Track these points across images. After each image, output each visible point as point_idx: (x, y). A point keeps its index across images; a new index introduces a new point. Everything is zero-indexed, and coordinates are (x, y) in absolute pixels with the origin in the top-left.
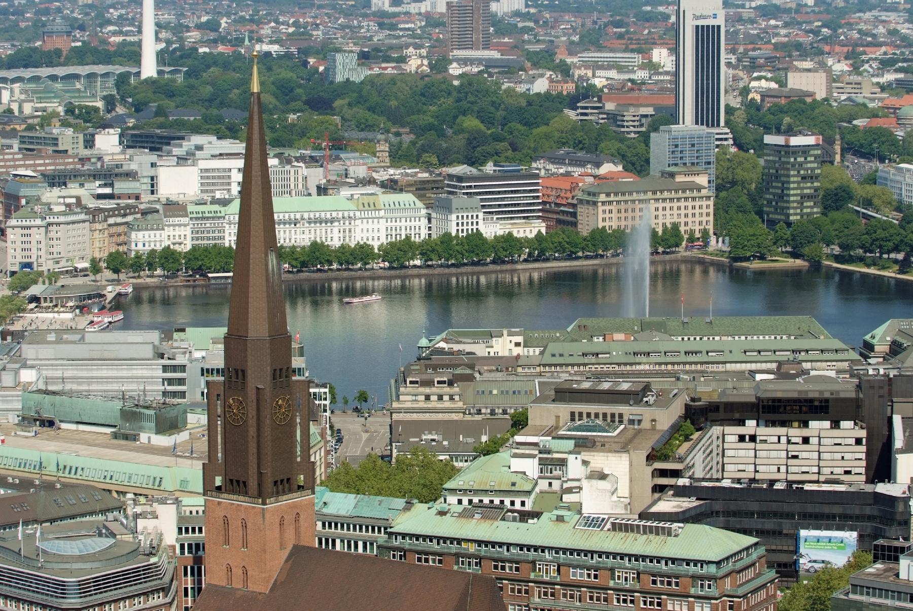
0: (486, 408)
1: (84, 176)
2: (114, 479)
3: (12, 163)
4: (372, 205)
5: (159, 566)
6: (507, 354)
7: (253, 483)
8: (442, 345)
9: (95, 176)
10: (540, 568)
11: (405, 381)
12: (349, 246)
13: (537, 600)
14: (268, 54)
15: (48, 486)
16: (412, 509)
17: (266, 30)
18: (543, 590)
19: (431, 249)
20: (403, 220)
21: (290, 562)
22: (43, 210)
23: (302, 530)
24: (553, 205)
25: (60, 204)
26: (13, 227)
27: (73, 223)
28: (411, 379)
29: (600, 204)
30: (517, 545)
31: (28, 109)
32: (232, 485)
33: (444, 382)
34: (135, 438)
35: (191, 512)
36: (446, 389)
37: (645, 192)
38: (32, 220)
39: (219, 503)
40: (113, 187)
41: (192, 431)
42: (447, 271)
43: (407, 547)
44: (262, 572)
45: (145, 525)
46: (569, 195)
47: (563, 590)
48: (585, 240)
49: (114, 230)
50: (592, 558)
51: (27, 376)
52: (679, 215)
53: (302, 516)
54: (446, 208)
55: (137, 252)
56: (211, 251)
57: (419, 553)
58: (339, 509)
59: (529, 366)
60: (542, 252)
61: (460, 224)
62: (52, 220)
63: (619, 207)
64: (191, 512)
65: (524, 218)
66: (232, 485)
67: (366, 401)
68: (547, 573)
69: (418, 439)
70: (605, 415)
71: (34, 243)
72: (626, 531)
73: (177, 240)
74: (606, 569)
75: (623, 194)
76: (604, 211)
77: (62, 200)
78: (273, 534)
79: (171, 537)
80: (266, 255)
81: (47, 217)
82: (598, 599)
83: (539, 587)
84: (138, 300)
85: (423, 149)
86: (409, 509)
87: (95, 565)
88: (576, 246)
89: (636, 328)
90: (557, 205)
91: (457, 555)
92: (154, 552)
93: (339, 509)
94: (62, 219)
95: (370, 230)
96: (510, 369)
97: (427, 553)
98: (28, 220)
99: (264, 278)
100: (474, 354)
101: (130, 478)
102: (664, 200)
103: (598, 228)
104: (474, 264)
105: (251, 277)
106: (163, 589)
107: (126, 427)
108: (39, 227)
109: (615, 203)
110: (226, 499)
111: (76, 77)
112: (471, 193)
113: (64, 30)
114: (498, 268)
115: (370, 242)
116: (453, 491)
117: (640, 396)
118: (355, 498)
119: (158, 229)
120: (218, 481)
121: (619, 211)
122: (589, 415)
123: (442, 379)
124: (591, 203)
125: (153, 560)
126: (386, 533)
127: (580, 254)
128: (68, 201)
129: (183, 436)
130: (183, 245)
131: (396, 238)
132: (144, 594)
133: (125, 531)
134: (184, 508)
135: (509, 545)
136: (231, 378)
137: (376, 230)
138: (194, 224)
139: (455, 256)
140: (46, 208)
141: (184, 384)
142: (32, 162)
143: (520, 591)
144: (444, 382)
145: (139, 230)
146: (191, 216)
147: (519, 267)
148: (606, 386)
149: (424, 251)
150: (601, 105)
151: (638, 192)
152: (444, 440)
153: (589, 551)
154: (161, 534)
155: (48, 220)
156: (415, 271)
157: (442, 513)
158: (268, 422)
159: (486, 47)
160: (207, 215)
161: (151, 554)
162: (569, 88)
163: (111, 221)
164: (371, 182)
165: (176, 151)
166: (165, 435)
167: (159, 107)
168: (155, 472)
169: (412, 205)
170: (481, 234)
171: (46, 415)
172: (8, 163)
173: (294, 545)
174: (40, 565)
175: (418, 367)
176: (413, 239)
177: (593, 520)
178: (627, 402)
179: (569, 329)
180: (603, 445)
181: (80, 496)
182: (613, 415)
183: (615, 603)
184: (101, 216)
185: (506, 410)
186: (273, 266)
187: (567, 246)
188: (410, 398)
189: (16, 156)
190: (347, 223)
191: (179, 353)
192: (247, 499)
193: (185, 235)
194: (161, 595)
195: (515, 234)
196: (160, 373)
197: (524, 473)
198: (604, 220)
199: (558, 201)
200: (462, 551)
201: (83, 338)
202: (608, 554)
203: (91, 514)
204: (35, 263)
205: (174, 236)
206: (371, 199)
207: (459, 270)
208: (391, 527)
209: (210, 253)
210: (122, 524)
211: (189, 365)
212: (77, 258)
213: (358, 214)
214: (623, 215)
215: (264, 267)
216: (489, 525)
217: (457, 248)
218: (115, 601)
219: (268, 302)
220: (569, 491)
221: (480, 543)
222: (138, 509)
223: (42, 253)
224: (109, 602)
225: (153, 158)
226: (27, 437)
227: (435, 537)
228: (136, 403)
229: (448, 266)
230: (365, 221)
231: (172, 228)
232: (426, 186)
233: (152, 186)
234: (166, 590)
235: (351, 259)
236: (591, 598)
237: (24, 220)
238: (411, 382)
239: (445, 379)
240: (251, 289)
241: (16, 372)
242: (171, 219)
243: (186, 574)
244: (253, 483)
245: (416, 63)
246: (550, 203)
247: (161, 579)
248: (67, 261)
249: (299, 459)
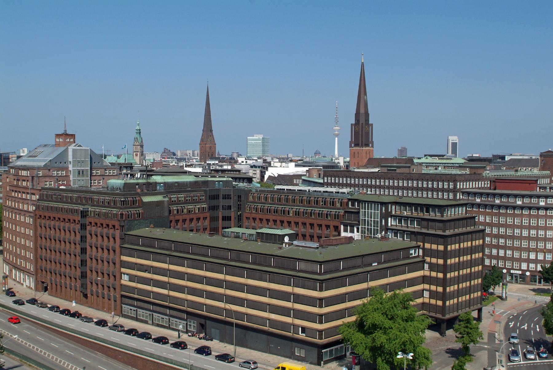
7: (360, 144)
78: (364, 155)
79: (342, 164)
120: (353, 145)
158: (364, 131)
173: (369, 158)
202: (437, 163)
244: (360, 144)
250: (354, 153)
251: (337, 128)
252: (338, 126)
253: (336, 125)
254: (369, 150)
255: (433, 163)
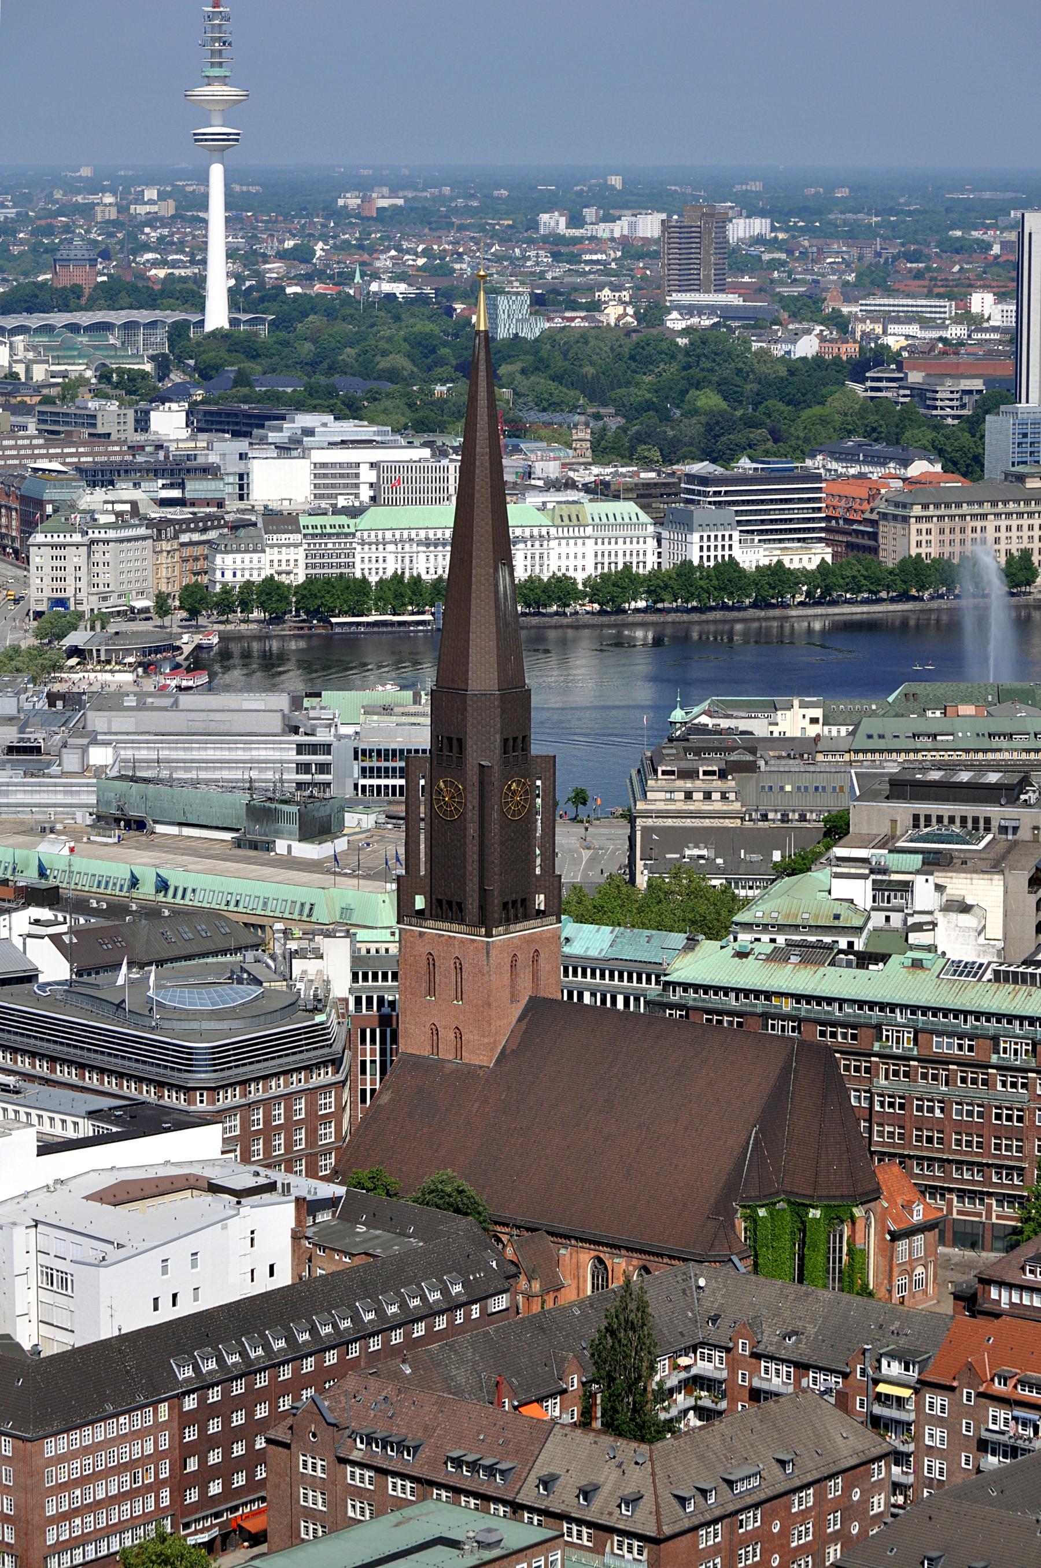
0: (776, 811)
1: (140, 471)
2: (241, 905)
3: (29, 452)
4: (574, 518)
5: (328, 1028)
6: (798, 734)
7: (472, 905)
8: (704, 719)
9: (156, 472)
10: (887, 1037)
11: (655, 772)
12: (540, 579)
13: (883, 1082)
14: (391, 297)
15: (152, 912)
16: (697, 949)
17: (384, 262)
18: (892, 1067)
19: (662, 584)
20: (621, 541)
21: (526, 1021)
22: (83, 521)
23: (543, 975)
24: (841, 522)
25: (106, 512)
26: (39, 546)
27: (129, 540)
28: (664, 768)
29: (913, 520)
30: (854, 1001)
31: (39, 373)
32: (441, 909)
33: (713, 773)
34: (269, 847)
35: (368, 951)
36: (717, 783)
37: (981, 503)
38: (68, 535)
39: (421, 934)
40: (183, 489)
41: (351, 838)
42: (685, 617)
43: (691, 1003)
44: (484, 1036)
45: (305, 968)
46: (866, 506)
47: (922, 1067)
48: (891, 573)
49: (187, 552)
50: (965, 1021)
51: (99, 756)
52: (1031, 538)
53: (542, 955)
54: (685, 524)
55: (224, 585)
56: (335, 584)
57: (709, 1012)
58: (588, 948)
59: (834, 752)
60: (827, 590)
61: (705, 548)
62: (97, 535)
63: (941, 524)
64: (368, 951)
65: (799, 540)
66: (441, 909)
67: (584, 803)
68: (898, 1043)
69: (678, 856)
70: (964, 820)
71: (70, 569)
72: (1015, 982)
73: (284, 567)
74: (985, 1037)
75: (948, 505)
76: (919, 532)
77: (109, 507)
78: (500, 980)
79: (341, 987)
80: (496, 571)
81: (90, 531)
82: (974, 1081)
83: (887, 1064)
84: (225, 655)
85: (640, 438)
86: (693, 949)
87: (235, 1024)
88: (878, 582)
89: (990, 698)
90: (846, 520)
91: (765, 1016)
92: (320, 1006)
93: (588, 948)
94: (112, 534)
95: (572, 556)
96: (806, 756)
97: (720, 1013)
98: (62, 535)
99: (492, 604)
100: (751, 733)
101: (265, 904)
102: (1009, 515)
103: (910, 556)
104: (725, 607)
105: (473, 602)
106: (333, 1062)
107: (254, 830)
108: (77, 546)
109: (935, 519)
110: (432, 929)
111: (107, 327)
112: (720, 502)
113: (86, 257)
114: (762, 614)
115: (571, 573)
116: (747, 926)
117: (1016, 791)
118: (612, 932)
119: (255, 551)
120: (420, 902)
121: (942, 531)
122: (940, 819)
123: (710, 768)
124: (900, 518)
125: (319, 1018)
126: (658, 983)
127: (883, 595)
128: (119, 507)
129: (341, 844)
130: (292, 576)
131: (610, 568)
132: (305, 1068)
133: (276, 977)
134: (358, 945)
135: (842, 1001)
136: (441, 751)
137: (580, 556)
138: (309, 544)
139: (699, 595)
140: (88, 518)
141: (329, 772)
142: (59, 451)
143: (857, 1069)
144: (713, 773)
145: (227, 552)
146: (304, 531)
147: (793, 613)
148: (965, 777)
149: (652, 588)
150: (902, 375)
151: (969, 503)
152: (716, 857)
153: (962, 1012)
154: (328, 982)
155: (91, 535)
156: (639, 618)
157: (742, 955)
159: (721, 289)
160: (328, 530)
161: (316, 1010)
162: (849, 350)
163: (185, 538)
164: (570, 485)
165: (273, 436)
166: (313, 842)
167: (239, 372)
168: (303, 895)
169: (634, 519)
170: (737, 564)
171: (134, 813)
172: (22, 452)
173: (531, 998)
174: (154, 1024)
175: (674, 751)
176: (634, 569)
177: (965, 967)
178: (996, 801)
179: (890, 699)
180: (964, 863)
181: (199, 928)
182: (976, 820)
183: (999, 1088)
184: (170, 531)
185: (805, 815)
186: (505, 587)
187: (864, 582)
188: (661, 795)
189: (35, 442)
190: (537, 544)
191: (321, 726)
192: (463, 928)
193: (296, 561)
194: (330, 1069)
195: (787, 564)
196: (292, 755)
197: (851, 901)
198: (919, 544)
199: (848, 516)
200: (773, 1011)
201: (176, 703)
202: (989, 1016)
203: (215, 954)
204: (72, 600)
205: (280, 561)
206: (573, 509)
207: (704, 617)
208: (666, 975)
209: (334, 587)
210: (268, 966)
211: (335, 744)
212: (134, 593)
213: (553, 531)
214: (947, 537)
215: (492, 588)
216: (812, 973)
217: (701, 583)
218: (265, 1078)
219: (498, 639)
220: (918, 927)
221: (798, 998)
222: (293, 945)
223: (83, 584)
224: (256, 1080)
225: (242, 445)
226: (106, 844)
227: (733, 989)
228: (270, 795)
229: (688, 611)
230: (564, 542)
231: (276, 549)
232: (653, 491)
233: (241, 488)
234: (337, 1062)
235: (544, 597)
236: (964, 1080)
237: (55, 535)
238: (664, 773)
239: (715, 768)
240: (473, 620)
241: (84, 750)
242: (275, 537)
243: (363, 1041)
244: (472, 905)
245: (614, 313)
246: (836, 519)
247: (331, 1045)
248: (120, 596)
249: (538, 871)
250: (431, 961)
251: (218, 90)
252: (224, 80)
253: (216, 72)
254: (529, 940)
255: (957, 1013)
